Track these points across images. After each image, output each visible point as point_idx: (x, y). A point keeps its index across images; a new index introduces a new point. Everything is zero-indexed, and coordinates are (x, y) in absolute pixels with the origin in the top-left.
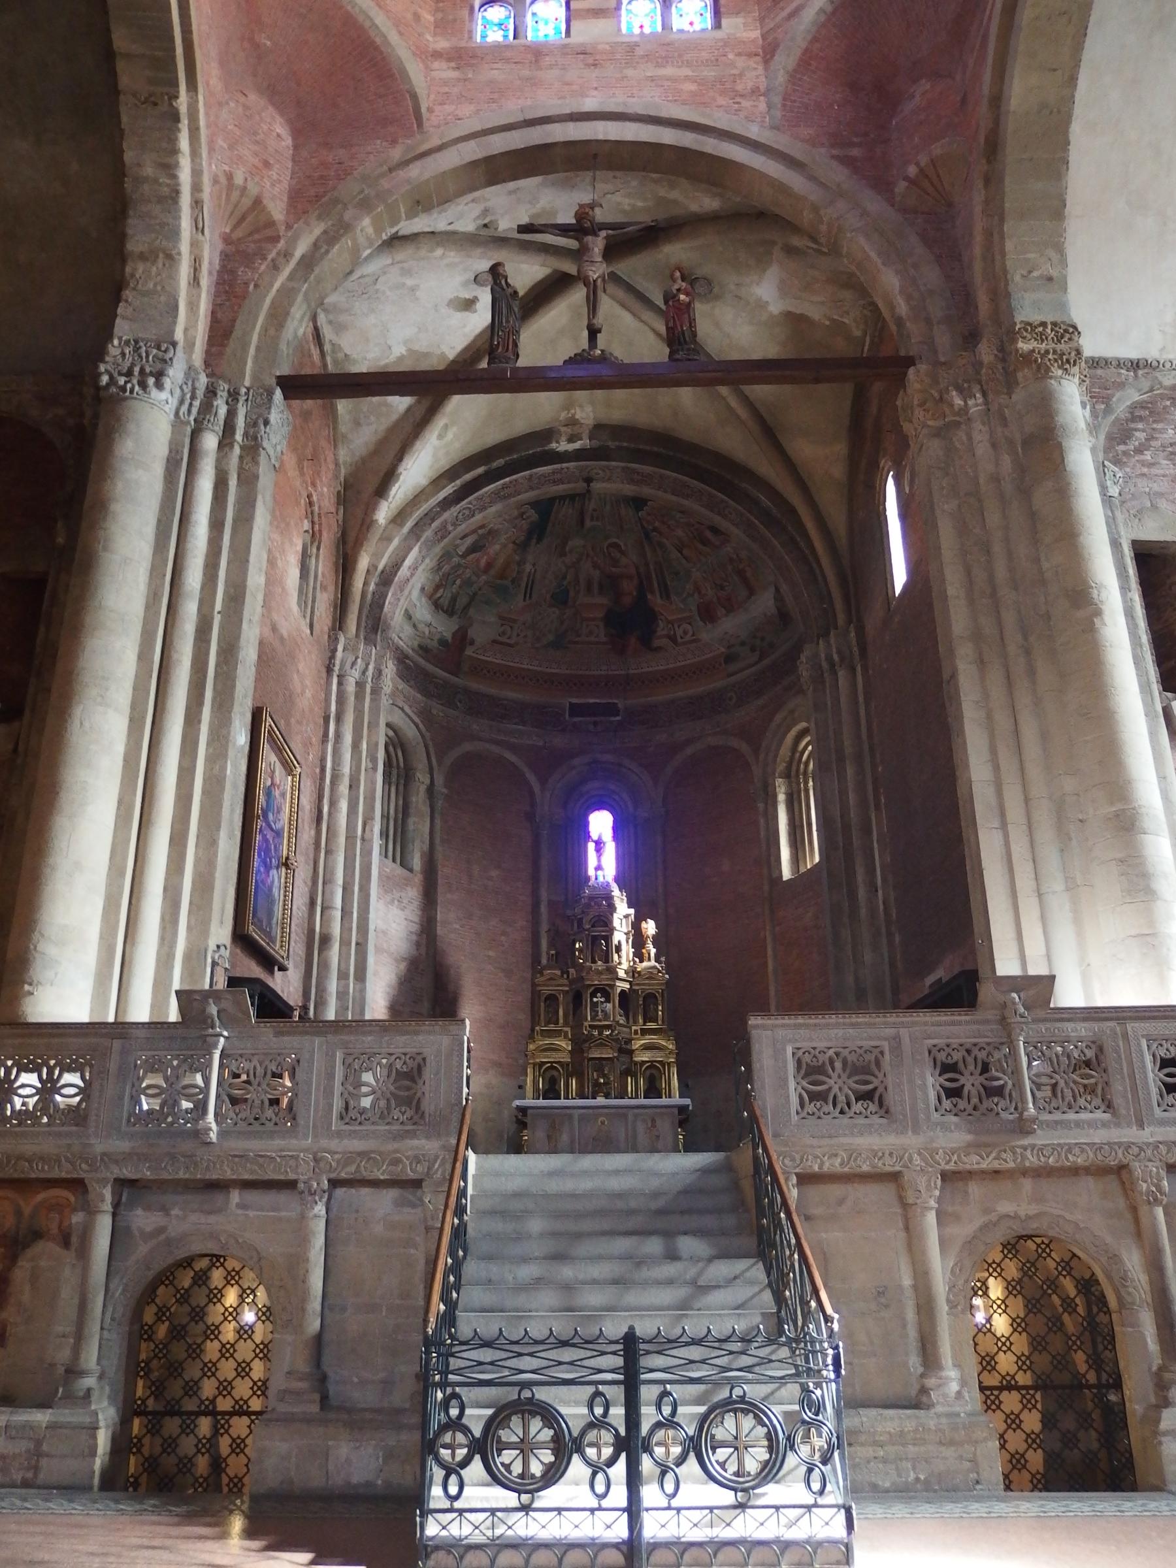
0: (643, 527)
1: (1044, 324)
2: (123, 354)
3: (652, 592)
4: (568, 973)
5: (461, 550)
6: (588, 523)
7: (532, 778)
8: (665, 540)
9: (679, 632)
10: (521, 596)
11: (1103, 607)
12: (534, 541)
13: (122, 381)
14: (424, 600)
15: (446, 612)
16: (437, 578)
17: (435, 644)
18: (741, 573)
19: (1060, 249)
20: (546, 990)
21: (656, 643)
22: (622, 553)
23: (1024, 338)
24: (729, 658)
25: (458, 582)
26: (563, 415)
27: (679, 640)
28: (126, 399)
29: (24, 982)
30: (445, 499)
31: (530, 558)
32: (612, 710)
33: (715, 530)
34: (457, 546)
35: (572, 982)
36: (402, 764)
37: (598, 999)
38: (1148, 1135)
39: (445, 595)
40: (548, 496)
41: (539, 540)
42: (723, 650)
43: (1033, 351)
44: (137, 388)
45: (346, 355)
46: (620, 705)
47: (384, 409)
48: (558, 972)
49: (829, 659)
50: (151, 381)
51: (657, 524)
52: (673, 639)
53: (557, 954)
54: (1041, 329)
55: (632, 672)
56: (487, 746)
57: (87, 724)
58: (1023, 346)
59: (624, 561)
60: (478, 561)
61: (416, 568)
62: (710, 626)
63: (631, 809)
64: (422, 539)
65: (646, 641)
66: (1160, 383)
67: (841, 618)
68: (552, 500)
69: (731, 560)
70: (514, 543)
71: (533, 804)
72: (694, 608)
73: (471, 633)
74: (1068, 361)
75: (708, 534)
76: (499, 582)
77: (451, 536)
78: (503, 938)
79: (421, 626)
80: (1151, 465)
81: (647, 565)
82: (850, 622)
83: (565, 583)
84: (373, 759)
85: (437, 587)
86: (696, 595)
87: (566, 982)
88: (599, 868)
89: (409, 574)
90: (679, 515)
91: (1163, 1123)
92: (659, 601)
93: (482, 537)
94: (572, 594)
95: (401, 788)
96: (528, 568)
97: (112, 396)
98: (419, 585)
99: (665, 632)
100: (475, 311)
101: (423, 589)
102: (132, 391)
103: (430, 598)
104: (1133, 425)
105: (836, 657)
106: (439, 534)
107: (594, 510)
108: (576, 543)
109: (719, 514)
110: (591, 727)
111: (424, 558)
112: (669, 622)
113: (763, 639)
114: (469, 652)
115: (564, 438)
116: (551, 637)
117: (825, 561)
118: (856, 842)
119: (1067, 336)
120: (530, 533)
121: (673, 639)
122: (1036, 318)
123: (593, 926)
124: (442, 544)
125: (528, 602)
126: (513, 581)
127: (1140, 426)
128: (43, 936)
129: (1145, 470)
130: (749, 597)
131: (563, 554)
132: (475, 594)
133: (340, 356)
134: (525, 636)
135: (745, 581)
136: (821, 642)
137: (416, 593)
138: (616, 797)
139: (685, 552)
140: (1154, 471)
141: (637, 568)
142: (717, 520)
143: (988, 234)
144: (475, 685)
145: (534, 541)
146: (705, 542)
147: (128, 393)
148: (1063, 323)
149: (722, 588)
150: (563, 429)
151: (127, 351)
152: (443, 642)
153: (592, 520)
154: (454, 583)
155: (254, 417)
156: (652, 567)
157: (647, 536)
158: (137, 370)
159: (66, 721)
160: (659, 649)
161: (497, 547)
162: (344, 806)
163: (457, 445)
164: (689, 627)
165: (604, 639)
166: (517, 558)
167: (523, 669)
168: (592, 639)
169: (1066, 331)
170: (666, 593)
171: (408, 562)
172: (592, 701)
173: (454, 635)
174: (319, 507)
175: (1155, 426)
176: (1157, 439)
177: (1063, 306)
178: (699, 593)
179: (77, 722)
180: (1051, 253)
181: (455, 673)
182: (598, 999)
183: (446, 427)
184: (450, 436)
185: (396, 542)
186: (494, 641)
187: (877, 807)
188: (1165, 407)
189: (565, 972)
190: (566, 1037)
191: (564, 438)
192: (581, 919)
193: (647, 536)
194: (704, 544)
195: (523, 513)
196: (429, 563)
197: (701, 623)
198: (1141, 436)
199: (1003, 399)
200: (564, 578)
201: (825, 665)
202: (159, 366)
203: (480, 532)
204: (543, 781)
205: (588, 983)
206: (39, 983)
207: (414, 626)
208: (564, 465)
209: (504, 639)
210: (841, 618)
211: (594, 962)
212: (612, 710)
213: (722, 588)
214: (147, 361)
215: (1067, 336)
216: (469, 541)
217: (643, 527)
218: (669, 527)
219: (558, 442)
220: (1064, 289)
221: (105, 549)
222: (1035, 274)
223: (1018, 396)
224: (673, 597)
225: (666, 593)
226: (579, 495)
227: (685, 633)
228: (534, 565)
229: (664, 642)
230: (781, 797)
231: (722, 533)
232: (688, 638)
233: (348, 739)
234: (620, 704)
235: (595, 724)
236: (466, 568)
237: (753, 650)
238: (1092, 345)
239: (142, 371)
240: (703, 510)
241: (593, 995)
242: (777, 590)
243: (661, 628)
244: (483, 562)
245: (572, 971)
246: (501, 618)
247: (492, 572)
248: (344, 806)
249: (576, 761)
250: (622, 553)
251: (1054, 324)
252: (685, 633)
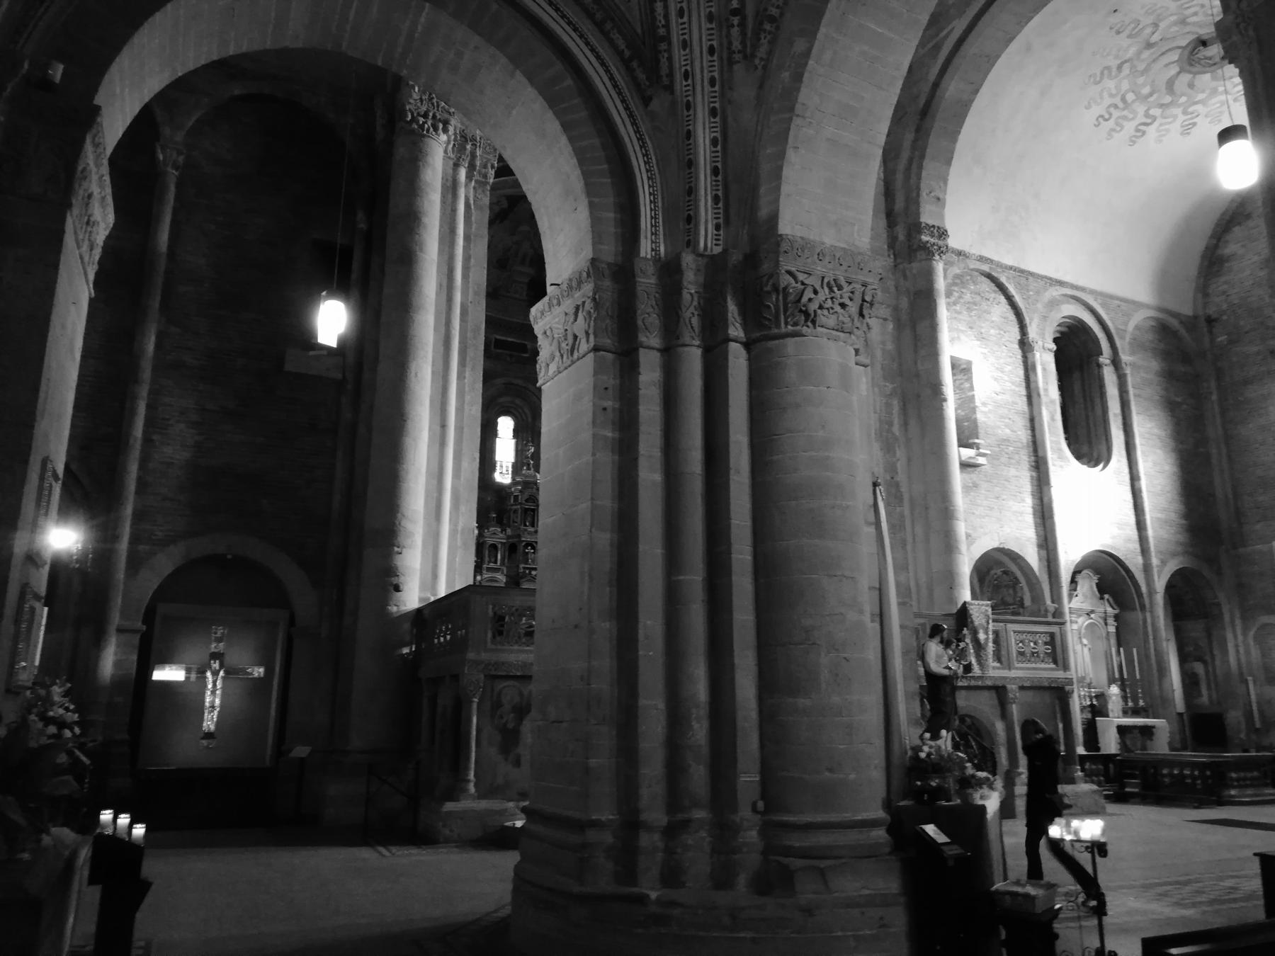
1: (933, 226)
2: (421, 100)
4: (505, 530)
11: (947, 397)
13: (421, 120)
19: (945, 181)
20: (490, 541)
23: (925, 233)
28: (424, 136)
29: (394, 545)
38: (1013, 674)
43: (928, 242)
44: (431, 129)
46: (529, 347)
50: (441, 126)
54: (932, 229)
57: (419, 375)
58: (925, 238)
63: (530, 420)
66: (968, 266)
74: (942, 252)
80: (959, 313)
87: (505, 537)
91: (1017, 669)
97: (413, 131)
102: (428, 130)
104: (953, 288)
119: (944, 236)
122: (931, 222)
127: (956, 289)
128: (404, 516)
129: (956, 315)
138: (520, 411)
140: (960, 317)
143: (911, 161)
147: (425, 132)
148: (943, 228)
151: (424, 98)
155: (485, 160)
158: (431, 114)
159: (407, 372)
169: (943, 233)
175: (962, 290)
176: (963, 298)
177: (942, 217)
179: (413, 374)
180: (942, 185)
188: (967, 280)
190: (502, 573)
198: (956, 294)
199: (906, 265)
202: (446, 116)
205: (524, 539)
206: (404, 547)
214: (438, 110)
215: (944, 236)
220: (943, 206)
221: (421, 250)
222: (932, 194)
223: (915, 265)
238: (953, 242)
239: (434, 117)
251: (938, 227)
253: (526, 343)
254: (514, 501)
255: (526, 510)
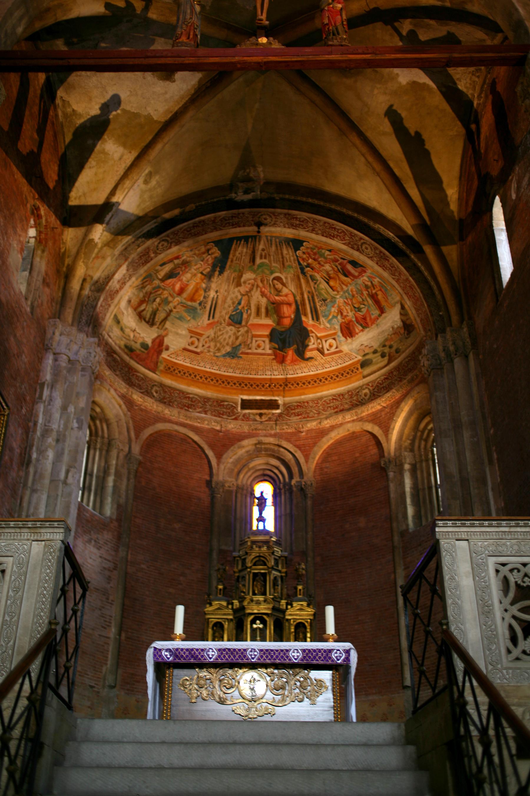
0: (300, 264)
3: (306, 315)
4: (232, 604)
5: (161, 275)
6: (258, 261)
7: (210, 453)
8: (316, 274)
9: (326, 346)
10: (206, 316)
12: (217, 273)
14: (130, 310)
15: (148, 322)
16: (141, 295)
17: (138, 346)
18: (374, 297)
21: (308, 354)
22: (284, 284)
24: (364, 364)
25: (158, 300)
26: (241, 173)
27: (326, 352)
30: (148, 231)
31: (214, 286)
32: (273, 405)
33: (354, 264)
34: (157, 271)
35: (235, 611)
36: (106, 435)
37: (258, 625)
39: (148, 309)
40: (228, 237)
41: (221, 273)
42: (360, 358)
45: (73, 110)
47: (102, 156)
48: (224, 603)
49: (446, 350)
51: (310, 261)
52: (321, 351)
53: (225, 588)
55: (289, 376)
56: (176, 427)
59: (285, 291)
60: (174, 285)
61: (124, 283)
62: (349, 340)
64: (130, 260)
65: (301, 354)
67: (455, 319)
68: (231, 241)
69: (367, 287)
70: (202, 273)
71: (211, 474)
72: (338, 327)
73: (166, 341)
75: (349, 267)
76: (189, 303)
77: (152, 262)
78: (181, 578)
79: (127, 331)
81: (302, 294)
82: (462, 321)
83: (240, 307)
84: (79, 421)
85: (141, 302)
86: (339, 317)
87: (231, 611)
88: (261, 519)
89: (118, 286)
90: (327, 253)
92: (311, 322)
93: (177, 266)
94: (245, 316)
95: (104, 452)
96: (212, 294)
98: (126, 298)
99: (315, 346)
100: (174, 81)
101: (129, 301)
103: (135, 309)
105: (452, 348)
106: (144, 259)
107: (263, 250)
108: (248, 276)
109: (358, 250)
110: (258, 418)
111: (130, 277)
112: (318, 338)
113: (391, 347)
114: (165, 355)
115: (241, 190)
116: (228, 349)
117: (441, 278)
118: (474, 492)
120: (214, 267)
121: (321, 351)
123: (255, 564)
124: (146, 268)
125: (211, 320)
126: (200, 304)
130: (380, 315)
131: (239, 285)
132: (171, 311)
133: (69, 110)
134: (209, 347)
135: (377, 302)
136: (439, 338)
137: (123, 304)
139: (332, 283)
141: (294, 297)
142: (356, 255)
144: (168, 381)
145: (217, 273)
146: (346, 274)
149: (359, 309)
150: (240, 184)
152: (144, 345)
153: (261, 258)
154: (154, 300)
156: (306, 296)
157: (303, 273)
160: (311, 358)
161: (188, 275)
162: (51, 454)
163: (159, 191)
164: (333, 341)
165: (270, 352)
166: (204, 285)
167: (207, 372)
168: (260, 351)
170: (316, 316)
171: (117, 276)
172: (258, 398)
173: (154, 341)
174: (46, 220)
178: (342, 314)
181: (154, 371)
182: (258, 625)
183: (150, 175)
184: (153, 182)
185: (108, 260)
186: (185, 349)
187: (491, 462)
189: (230, 603)
191: (241, 190)
192: (245, 559)
193: (302, 269)
194: (346, 276)
195: (208, 250)
196: (135, 281)
197: (343, 339)
200: (239, 303)
201: (442, 355)
203: (176, 261)
204: (219, 456)
205: (248, 611)
207: (122, 329)
208: (241, 211)
209: (192, 348)
210: (455, 319)
211: (254, 594)
212: (273, 405)
213: (359, 309)
216: (167, 268)
217: (300, 264)
218: (319, 263)
219: (236, 193)
224: (322, 319)
225: (316, 316)
226: (252, 237)
227: (331, 346)
228: (217, 292)
229: (315, 353)
230: (407, 467)
231: (361, 266)
232: (333, 350)
233: (58, 402)
234: (280, 400)
235: (261, 415)
236: (164, 290)
237: (383, 356)
240: (344, 247)
241: (253, 622)
242: (403, 307)
243: (312, 343)
244: (178, 287)
245: (236, 603)
246: (191, 331)
247: (185, 295)
248: (51, 454)
249: (245, 442)
250: (284, 284)
252: (331, 346)
253: (277, 398)
254: (242, 566)
255: (255, 575)
